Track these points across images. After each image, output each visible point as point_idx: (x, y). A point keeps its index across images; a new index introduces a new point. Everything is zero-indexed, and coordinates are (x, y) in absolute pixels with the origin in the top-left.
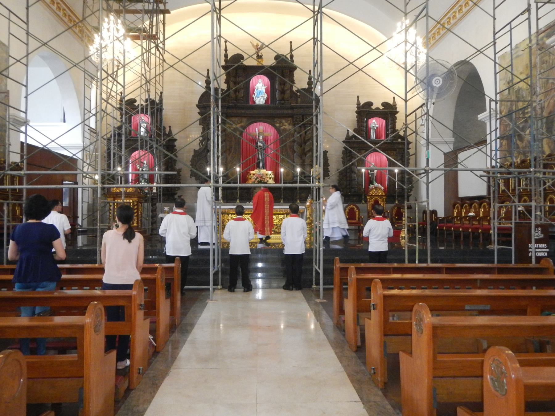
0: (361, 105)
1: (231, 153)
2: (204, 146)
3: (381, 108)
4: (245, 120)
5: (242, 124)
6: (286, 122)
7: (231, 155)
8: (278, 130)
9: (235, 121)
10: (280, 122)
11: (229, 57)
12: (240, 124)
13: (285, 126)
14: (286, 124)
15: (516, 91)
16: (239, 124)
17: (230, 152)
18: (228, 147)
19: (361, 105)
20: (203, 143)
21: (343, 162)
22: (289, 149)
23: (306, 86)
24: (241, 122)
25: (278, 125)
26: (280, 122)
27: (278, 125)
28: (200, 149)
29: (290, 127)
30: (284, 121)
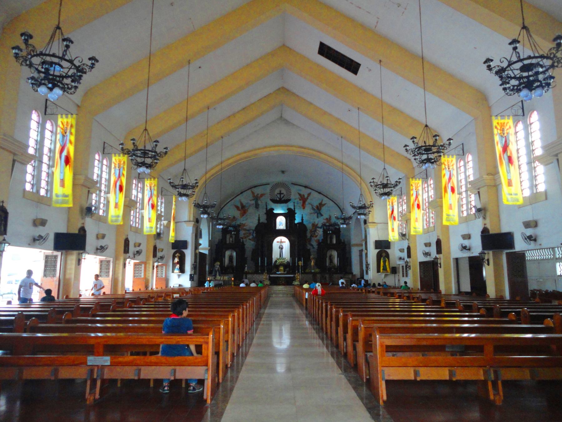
23: (300, 221)
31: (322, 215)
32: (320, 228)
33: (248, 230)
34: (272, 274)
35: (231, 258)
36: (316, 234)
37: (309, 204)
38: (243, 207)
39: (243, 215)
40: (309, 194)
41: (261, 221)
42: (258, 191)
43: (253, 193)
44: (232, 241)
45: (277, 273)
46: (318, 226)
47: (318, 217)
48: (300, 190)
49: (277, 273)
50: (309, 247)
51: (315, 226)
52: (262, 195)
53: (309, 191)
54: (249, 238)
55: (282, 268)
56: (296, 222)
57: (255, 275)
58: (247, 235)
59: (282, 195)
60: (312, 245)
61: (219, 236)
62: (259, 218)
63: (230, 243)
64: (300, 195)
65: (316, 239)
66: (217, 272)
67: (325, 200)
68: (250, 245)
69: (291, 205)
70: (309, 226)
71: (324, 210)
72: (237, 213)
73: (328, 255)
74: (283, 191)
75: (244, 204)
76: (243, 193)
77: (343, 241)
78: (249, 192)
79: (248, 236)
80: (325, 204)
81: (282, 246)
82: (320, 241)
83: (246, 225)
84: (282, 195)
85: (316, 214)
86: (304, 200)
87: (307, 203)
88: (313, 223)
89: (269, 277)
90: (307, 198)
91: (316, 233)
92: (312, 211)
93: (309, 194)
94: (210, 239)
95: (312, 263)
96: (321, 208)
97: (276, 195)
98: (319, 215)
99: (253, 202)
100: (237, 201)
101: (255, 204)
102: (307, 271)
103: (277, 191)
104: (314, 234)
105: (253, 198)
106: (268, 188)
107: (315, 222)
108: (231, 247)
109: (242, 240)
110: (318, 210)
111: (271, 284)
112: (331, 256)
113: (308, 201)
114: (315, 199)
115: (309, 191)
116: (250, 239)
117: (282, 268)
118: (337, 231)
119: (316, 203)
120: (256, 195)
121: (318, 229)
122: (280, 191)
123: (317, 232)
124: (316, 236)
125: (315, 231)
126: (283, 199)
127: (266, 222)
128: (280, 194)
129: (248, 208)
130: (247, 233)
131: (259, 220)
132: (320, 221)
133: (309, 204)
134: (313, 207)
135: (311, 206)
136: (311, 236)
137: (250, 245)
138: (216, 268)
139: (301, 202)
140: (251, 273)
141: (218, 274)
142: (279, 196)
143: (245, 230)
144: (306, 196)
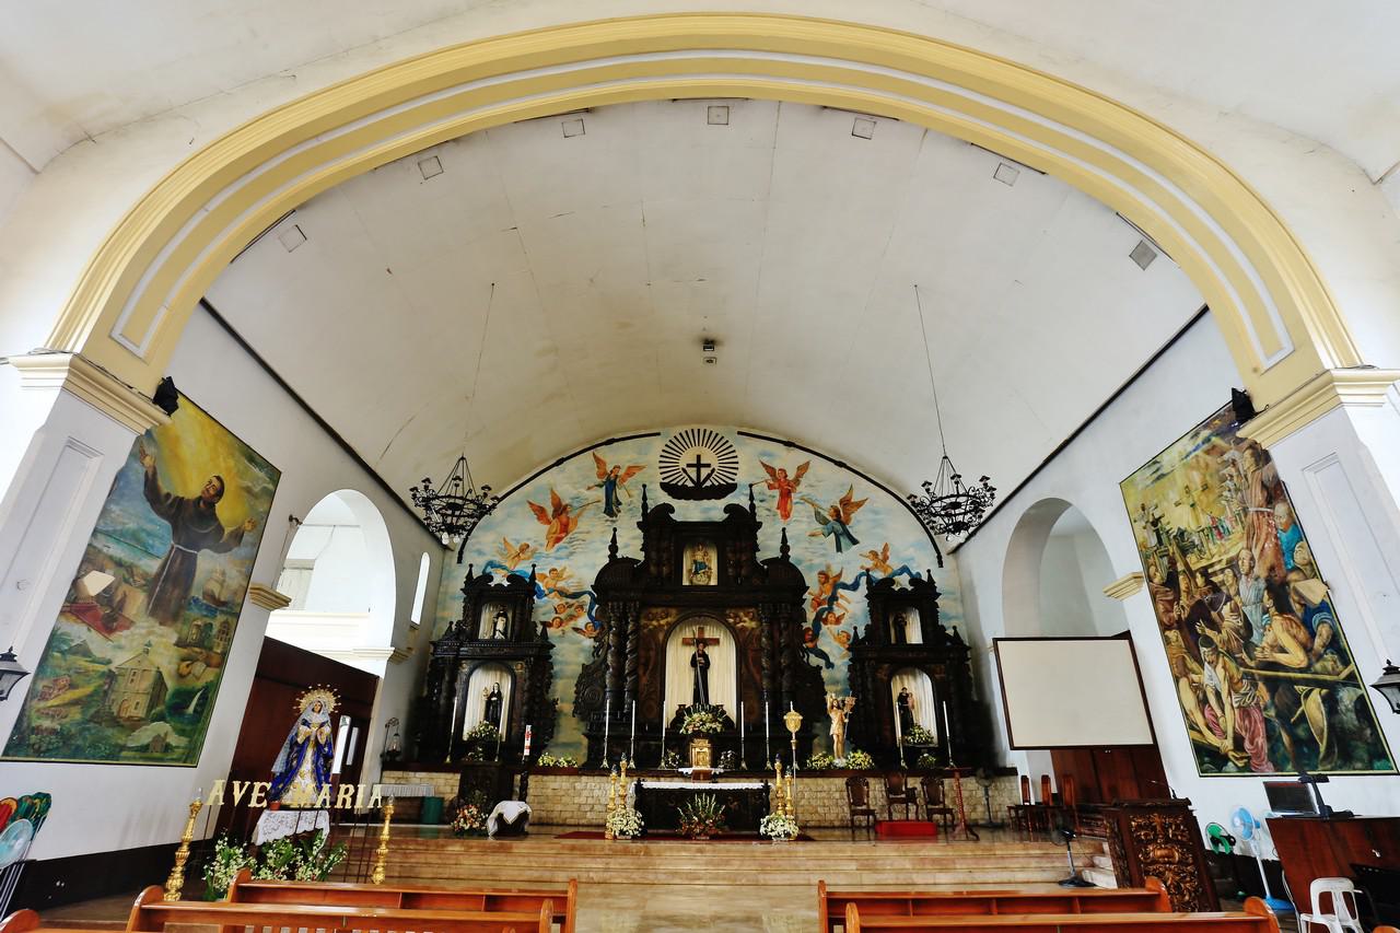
2: (602, 657)
4: (674, 611)
13: (745, 622)
14: (746, 619)
15: (1175, 537)
16: (663, 618)
18: (643, 660)
23: (779, 555)
25: (731, 620)
26: (736, 616)
27: (731, 620)
28: (594, 662)
29: (753, 624)
31: (855, 542)
32: (854, 587)
33: (576, 596)
34: (658, 775)
35: (492, 704)
36: (838, 612)
37: (805, 500)
38: (560, 509)
39: (558, 540)
40: (803, 469)
41: (619, 555)
42: (616, 457)
43: (598, 460)
44: (505, 633)
45: (684, 770)
46: (842, 580)
47: (839, 549)
48: (769, 455)
49: (684, 770)
50: (814, 661)
51: (834, 584)
52: (631, 471)
53: (801, 457)
54: (572, 624)
55: (706, 750)
56: (761, 556)
57: (584, 778)
59: (705, 472)
60: (823, 655)
61: (455, 612)
62: (614, 540)
63: (492, 640)
64: (770, 470)
65: (834, 628)
66: (300, 757)
67: (863, 489)
68: (573, 649)
69: (739, 499)
70: (812, 580)
71: (858, 524)
72: (535, 532)
73: (895, 696)
74: (709, 457)
75: (565, 501)
77: (950, 632)
79: (572, 617)
80: (859, 504)
81: (706, 657)
82: (861, 633)
84: (705, 472)
86: (785, 487)
87: (795, 497)
89: (639, 788)
90: (797, 481)
92: (818, 527)
93: (803, 469)
94: (416, 617)
95: (836, 729)
96: (848, 515)
97: (684, 470)
98: (844, 541)
99: (601, 493)
100: (539, 491)
102: (818, 760)
103: (688, 457)
104: (830, 610)
105: (599, 481)
106: (658, 445)
107: (828, 567)
108: (492, 658)
109: (540, 629)
110: (839, 524)
111: (644, 835)
112: (903, 698)
113: (802, 489)
114: (825, 485)
115: (803, 457)
116: (576, 630)
117: (701, 751)
118: (923, 594)
119: (829, 500)
120: (609, 470)
121: (841, 591)
122: (699, 457)
123: (840, 601)
124: (838, 621)
125: (833, 598)
126: (708, 483)
127: (641, 556)
128: (699, 465)
129: (579, 515)
131: (613, 548)
132: (850, 564)
133: (805, 500)
134: (817, 514)
135: (812, 509)
136: (819, 620)
137: (573, 649)
138: (303, 728)
139: (777, 493)
140: (570, 771)
141: (307, 766)
142: (692, 472)
143: (562, 593)
144: (791, 476)
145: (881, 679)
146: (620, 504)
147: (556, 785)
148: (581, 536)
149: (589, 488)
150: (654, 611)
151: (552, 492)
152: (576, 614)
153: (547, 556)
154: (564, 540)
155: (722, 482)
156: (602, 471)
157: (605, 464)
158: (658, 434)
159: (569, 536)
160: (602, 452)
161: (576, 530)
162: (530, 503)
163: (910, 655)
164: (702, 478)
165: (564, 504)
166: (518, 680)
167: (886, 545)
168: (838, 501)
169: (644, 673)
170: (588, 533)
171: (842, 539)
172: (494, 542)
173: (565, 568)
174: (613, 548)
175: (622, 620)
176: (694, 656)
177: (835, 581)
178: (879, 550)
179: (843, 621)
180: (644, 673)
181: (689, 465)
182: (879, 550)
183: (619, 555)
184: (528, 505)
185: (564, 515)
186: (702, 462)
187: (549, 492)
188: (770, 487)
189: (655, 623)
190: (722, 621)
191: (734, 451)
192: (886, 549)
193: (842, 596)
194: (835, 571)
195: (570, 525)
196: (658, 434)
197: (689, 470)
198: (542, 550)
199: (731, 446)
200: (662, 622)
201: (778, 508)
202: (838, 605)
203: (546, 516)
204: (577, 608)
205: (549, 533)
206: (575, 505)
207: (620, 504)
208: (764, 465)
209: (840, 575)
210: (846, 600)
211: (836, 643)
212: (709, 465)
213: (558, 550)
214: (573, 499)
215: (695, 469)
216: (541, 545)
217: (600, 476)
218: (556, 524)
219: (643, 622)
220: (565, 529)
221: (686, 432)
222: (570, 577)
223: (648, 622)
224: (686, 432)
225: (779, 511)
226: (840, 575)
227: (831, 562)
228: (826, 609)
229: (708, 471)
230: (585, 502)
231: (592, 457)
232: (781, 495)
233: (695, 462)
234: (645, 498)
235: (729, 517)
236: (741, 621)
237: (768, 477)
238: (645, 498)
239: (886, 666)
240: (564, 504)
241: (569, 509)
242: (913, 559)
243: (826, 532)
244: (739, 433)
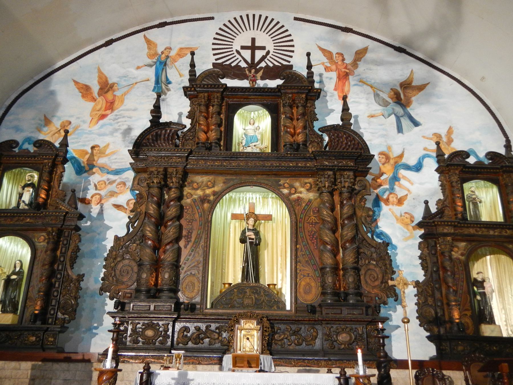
0: (446, 156)
1: (191, 244)
3: (487, 162)
4: (220, 179)
5: (216, 189)
6: (303, 185)
7: (189, 247)
8: (286, 199)
9: (202, 182)
10: (291, 187)
11: (199, 72)
12: (213, 189)
13: (301, 193)
14: (302, 189)
17: (188, 242)
19: (446, 156)
20: (135, 225)
21: (421, 264)
22: (308, 237)
24: (213, 187)
25: (285, 191)
26: (291, 187)
29: (311, 196)
30: (297, 184)
31: (416, 124)
32: (418, 168)
33: (117, 172)
36: (400, 192)
39: (103, 117)
40: (360, 54)
43: (148, 42)
46: (404, 161)
47: (400, 130)
53: (359, 42)
54: (113, 200)
55: (255, 333)
58: (113, 187)
59: (259, 54)
65: (398, 210)
76: (114, 44)
78: (139, 39)
79: (112, 194)
81: (257, 233)
82: (433, 209)
83: (108, 152)
84: (259, 54)
85: (393, 118)
88: (384, 149)
91: (396, 187)
98: (405, 123)
99: (151, 73)
101: (153, 79)
105: (149, 61)
107: (389, 148)
116: (118, 207)
120: (160, 50)
121: (403, 172)
122: (253, 40)
123: (402, 182)
124: (400, 202)
126: (263, 64)
128: (253, 48)
129: (125, 94)
130: (111, 182)
131: (156, 111)
139: (334, 75)
142: (247, 54)
145: (459, 259)
146: (170, 83)
147: (68, 376)
148: (127, 113)
149: (138, 68)
150: (199, 179)
151: (100, 71)
152: (116, 190)
153: (90, 133)
154: (109, 117)
155: (277, 64)
156: (152, 52)
157: (156, 45)
158: (212, 18)
159: (115, 112)
160: (153, 34)
161: (121, 109)
162: (74, 81)
163: (491, 233)
164: (257, 59)
165: (110, 82)
166: (39, 254)
167: (450, 128)
168: (398, 85)
169: (185, 247)
170: (135, 110)
171: (402, 120)
172: (34, 119)
173: (108, 145)
174: (156, 111)
175: (164, 186)
176: (244, 232)
177: (396, 163)
178: (443, 132)
179: (405, 203)
180: (185, 247)
181: (243, 48)
182: (443, 132)
183: (162, 121)
184: (73, 83)
185: (110, 93)
186: (257, 44)
187: (96, 70)
188: (327, 69)
189: (200, 192)
190: (275, 189)
191: (290, 35)
192: (450, 131)
193: (404, 177)
194: (396, 152)
195: (116, 103)
196: (212, 18)
197: (243, 52)
198: (85, 126)
199: (287, 31)
200: (208, 191)
201: (335, 89)
202: (400, 186)
203: (91, 93)
204: (119, 184)
205: (94, 110)
206: (123, 83)
207: (170, 83)
208: (319, 47)
209: (401, 156)
210: (409, 181)
211: (399, 225)
212: (263, 48)
213: (102, 126)
214: (119, 77)
215: (249, 52)
216: (84, 122)
217: (150, 56)
218: (101, 102)
219: (187, 190)
220: (111, 106)
221: (241, 17)
222: (113, 153)
223: (192, 192)
224: (241, 17)
225: (336, 93)
226: (401, 156)
227: (390, 143)
228: (387, 190)
229: (263, 53)
230: (134, 81)
231: (143, 39)
232: (339, 78)
233: (250, 44)
234: (193, 65)
235: (284, 83)
236: (296, 192)
237: (325, 60)
238: (193, 65)
239: (463, 244)
240: (110, 82)
241: (115, 88)
242: (480, 142)
243: (386, 114)
244: (296, 19)
